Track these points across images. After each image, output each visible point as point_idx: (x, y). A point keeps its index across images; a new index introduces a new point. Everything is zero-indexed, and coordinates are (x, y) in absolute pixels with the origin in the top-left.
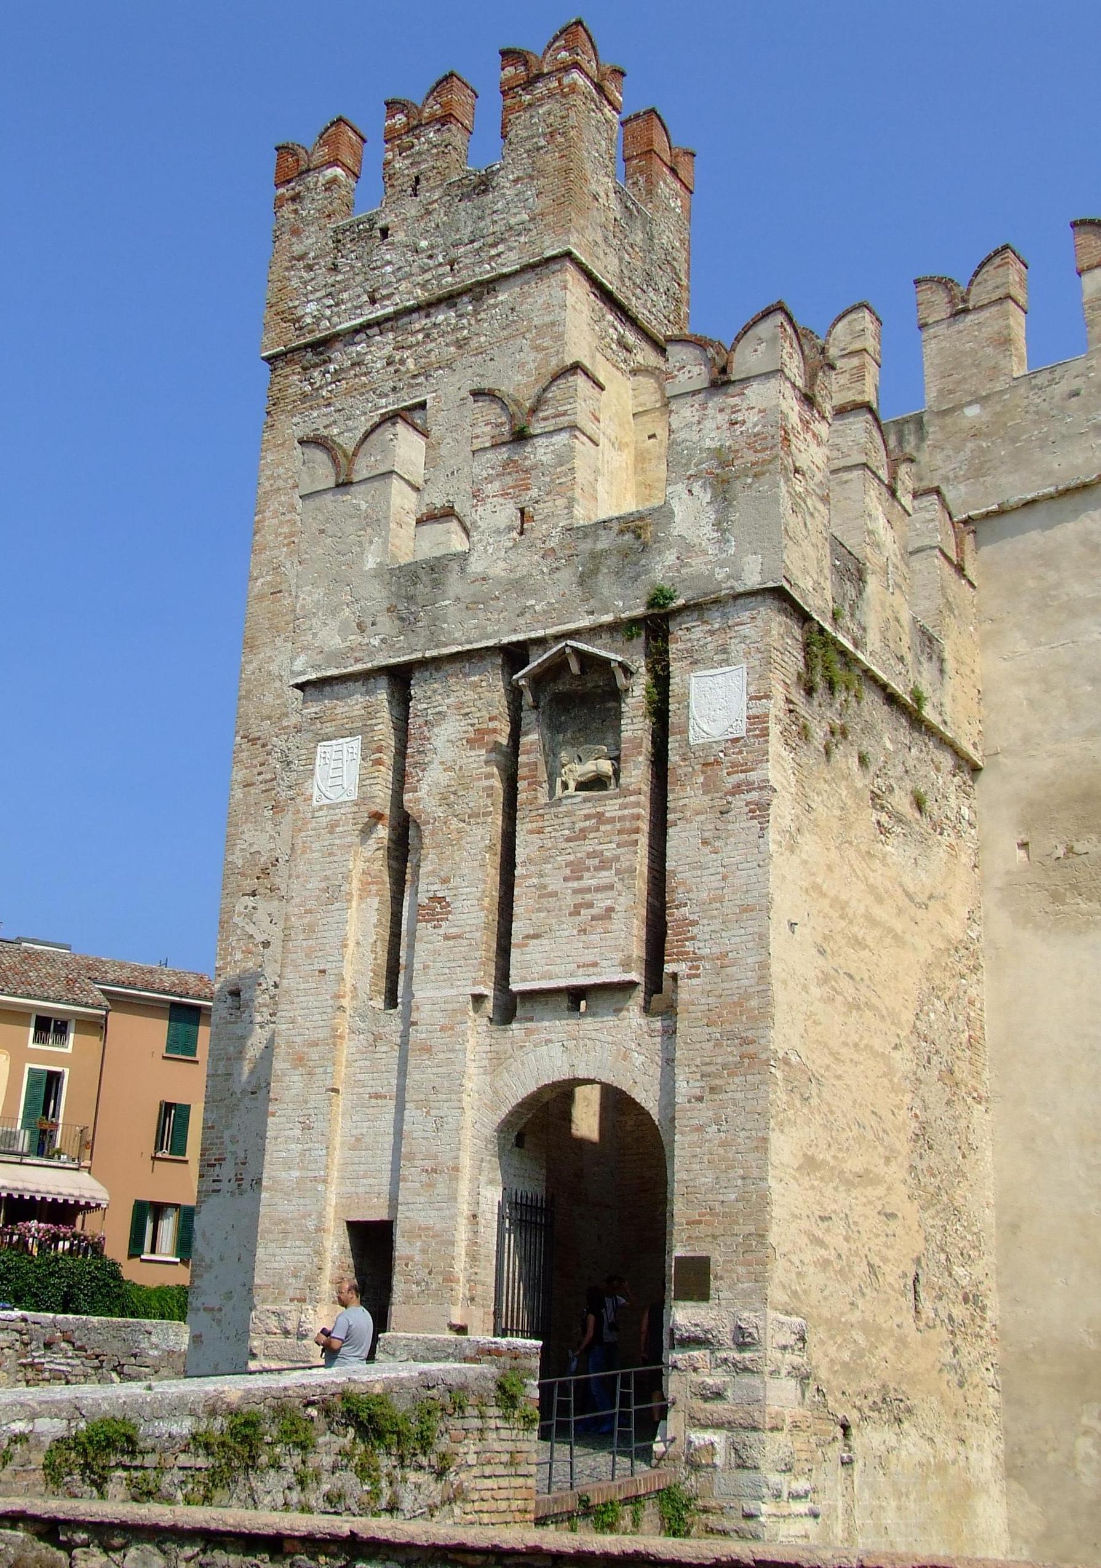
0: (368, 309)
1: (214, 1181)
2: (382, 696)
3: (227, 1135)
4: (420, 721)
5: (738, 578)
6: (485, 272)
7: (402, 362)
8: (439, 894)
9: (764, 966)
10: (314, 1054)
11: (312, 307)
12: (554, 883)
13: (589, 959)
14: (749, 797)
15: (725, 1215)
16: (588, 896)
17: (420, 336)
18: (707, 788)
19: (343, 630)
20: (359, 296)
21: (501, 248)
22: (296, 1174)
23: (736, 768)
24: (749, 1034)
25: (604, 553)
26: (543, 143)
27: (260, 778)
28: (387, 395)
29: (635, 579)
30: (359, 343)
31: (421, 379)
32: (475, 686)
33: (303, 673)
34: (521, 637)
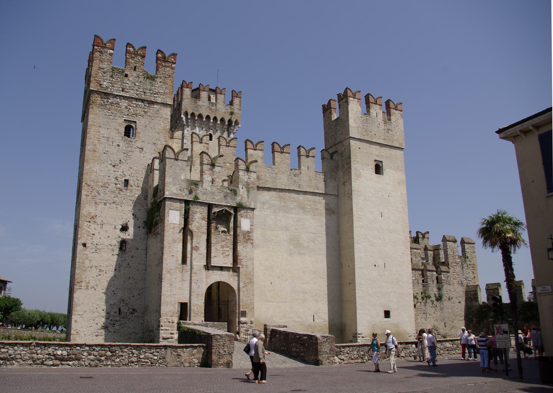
0: (122, 92)
4: (192, 212)
5: (251, 205)
6: (152, 99)
8: (197, 246)
9: (253, 268)
10: (172, 271)
11: (105, 83)
12: (219, 248)
13: (225, 262)
15: (248, 305)
16: (225, 252)
17: (135, 105)
19: (176, 189)
20: (119, 88)
21: (157, 96)
22: (169, 293)
24: (251, 278)
26: (167, 77)
27: (91, 195)
28: (125, 115)
29: (234, 199)
30: (118, 99)
31: (134, 116)
32: (203, 209)
33: (168, 195)
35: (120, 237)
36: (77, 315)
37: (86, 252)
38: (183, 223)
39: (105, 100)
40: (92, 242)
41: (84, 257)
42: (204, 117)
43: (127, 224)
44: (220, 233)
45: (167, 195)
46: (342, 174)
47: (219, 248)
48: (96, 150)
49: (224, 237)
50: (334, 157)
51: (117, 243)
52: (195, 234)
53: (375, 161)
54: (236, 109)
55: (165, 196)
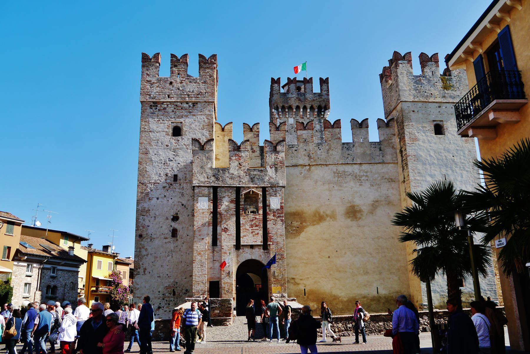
2: (212, 191)
3: (141, 263)
7: (176, 112)
10: (202, 253)
12: (248, 227)
14: (281, 218)
16: (254, 231)
18: (274, 216)
19: (204, 177)
21: (199, 96)
23: (278, 213)
25: (255, 175)
27: (145, 192)
30: (165, 105)
32: (231, 193)
33: (196, 184)
34: (241, 186)
35: (171, 226)
36: (136, 298)
37: (142, 243)
38: (212, 208)
39: (154, 108)
42: (294, 108)
43: (177, 214)
44: (249, 213)
45: (195, 184)
46: (399, 140)
47: (248, 227)
48: (147, 153)
49: (253, 216)
50: (390, 125)
52: (224, 217)
53: (434, 121)
54: (324, 95)
55: (193, 185)
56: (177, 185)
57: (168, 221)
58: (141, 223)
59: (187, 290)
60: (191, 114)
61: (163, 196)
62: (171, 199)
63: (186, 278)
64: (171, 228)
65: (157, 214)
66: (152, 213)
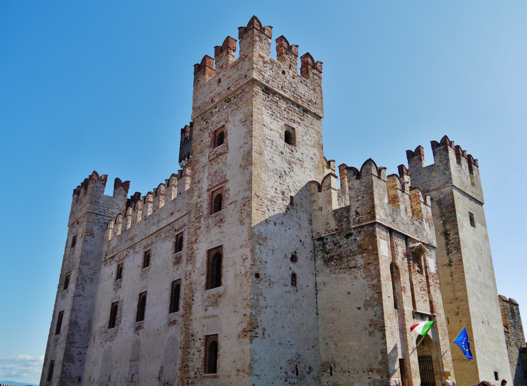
1: (256, 333)
3: (259, 319)
27: (261, 209)
35: (291, 269)
37: (260, 286)
40: (265, 273)
41: (258, 292)
43: (296, 253)
51: (289, 276)
56: (294, 210)
57: (287, 259)
58: (258, 255)
59: (310, 368)
60: (303, 122)
61: (281, 222)
62: (289, 229)
63: (308, 350)
64: (291, 272)
65: (276, 247)
66: (270, 242)
